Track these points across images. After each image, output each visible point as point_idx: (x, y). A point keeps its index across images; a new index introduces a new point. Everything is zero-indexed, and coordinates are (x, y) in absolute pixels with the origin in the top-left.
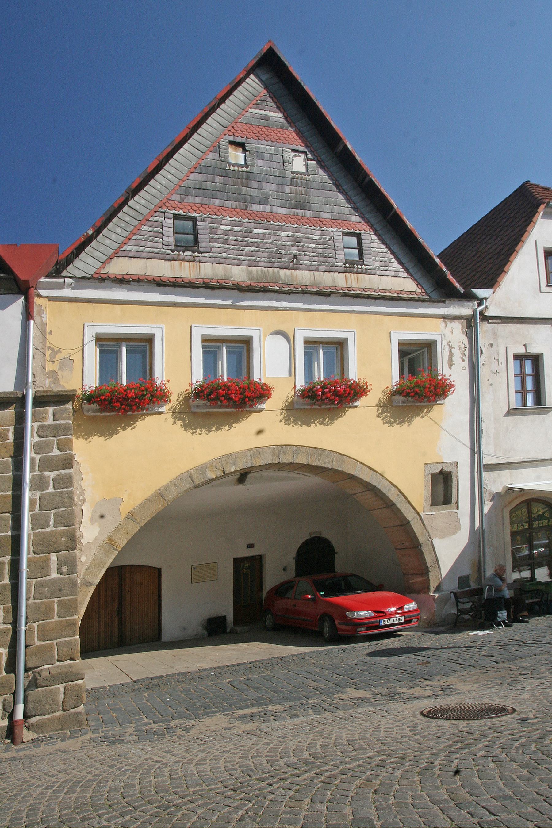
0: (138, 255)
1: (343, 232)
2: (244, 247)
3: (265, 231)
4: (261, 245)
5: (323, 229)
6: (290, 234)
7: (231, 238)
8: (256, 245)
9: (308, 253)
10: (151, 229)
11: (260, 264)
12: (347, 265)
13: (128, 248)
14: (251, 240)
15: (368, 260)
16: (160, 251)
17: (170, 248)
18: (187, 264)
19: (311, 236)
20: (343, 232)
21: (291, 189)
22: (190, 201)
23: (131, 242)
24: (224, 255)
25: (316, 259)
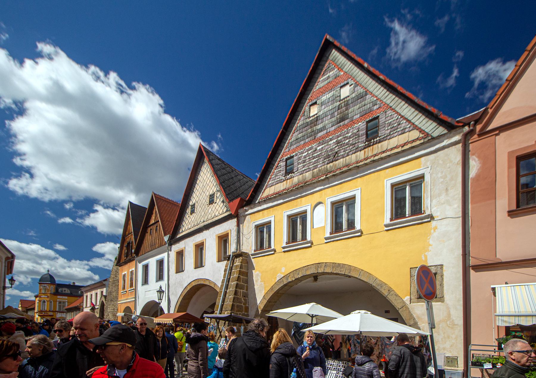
6: (335, 141)
10: (278, 170)
12: (367, 143)
13: (270, 183)
14: (316, 154)
18: (289, 181)
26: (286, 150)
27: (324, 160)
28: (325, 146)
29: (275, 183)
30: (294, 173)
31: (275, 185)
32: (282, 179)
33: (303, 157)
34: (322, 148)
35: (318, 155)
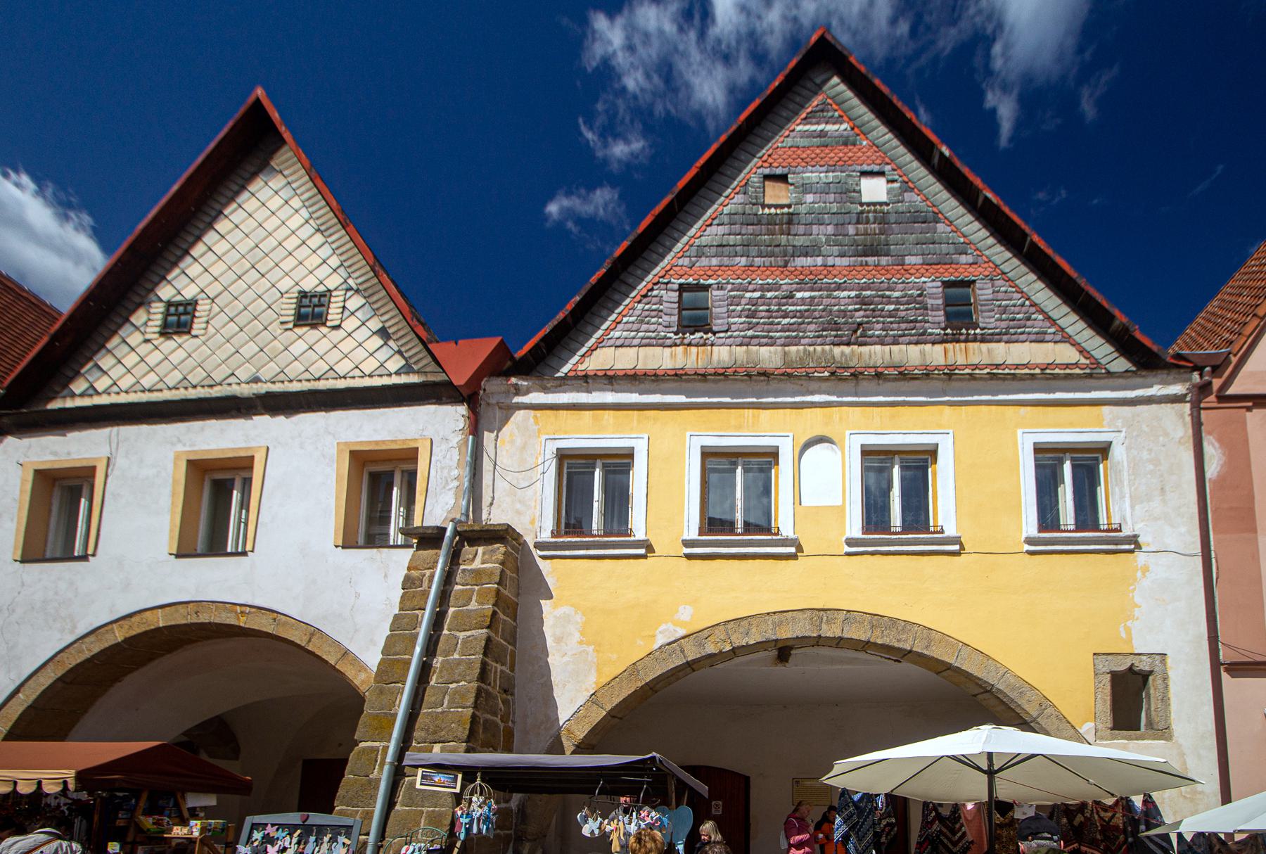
0: (627, 342)
1: (943, 283)
2: (779, 320)
3: (813, 294)
4: (806, 314)
5: (910, 280)
6: (853, 294)
7: (761, 308)
8: (798, 314)
9: (882, 319)
10: (647, 307)
11: (803, 341)
12: (949, 331)
14: (791, 308)
15: (987, 320)
16: (658, 335)
17: (671, 329)
18: (694, 349)
19: (887, 293)
20: (943, 283)
21: (857, 229)
22: (703, 265)
23: (620, 327)
24: (750, 333)
25: (895, 326)
26: (680, 262)
27: (823, 330)
28: (821, 297)
29: (636, 342)
30: (714, 333)
31: (640, 346)
32: (665, 338)
33: (743, 301)
34: (812, 298)
35: (800, 311)
